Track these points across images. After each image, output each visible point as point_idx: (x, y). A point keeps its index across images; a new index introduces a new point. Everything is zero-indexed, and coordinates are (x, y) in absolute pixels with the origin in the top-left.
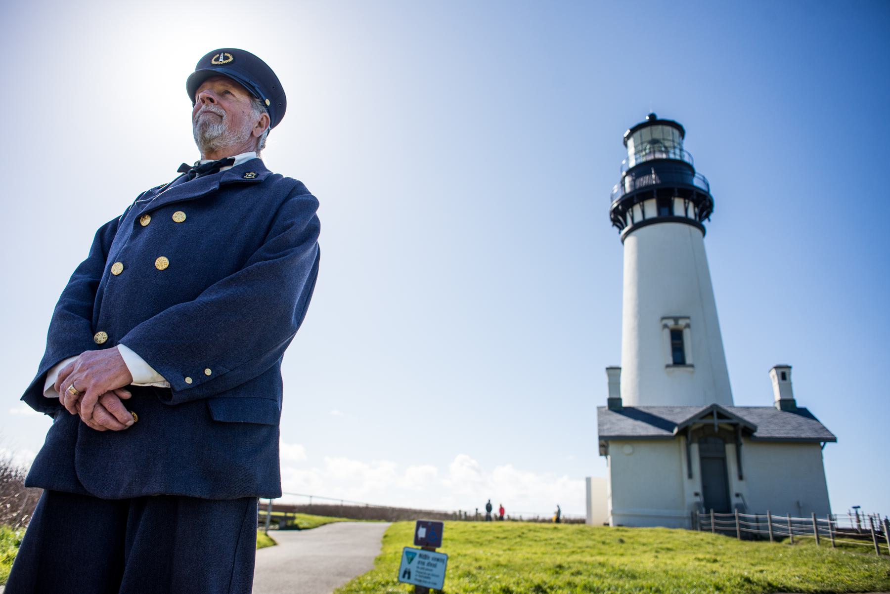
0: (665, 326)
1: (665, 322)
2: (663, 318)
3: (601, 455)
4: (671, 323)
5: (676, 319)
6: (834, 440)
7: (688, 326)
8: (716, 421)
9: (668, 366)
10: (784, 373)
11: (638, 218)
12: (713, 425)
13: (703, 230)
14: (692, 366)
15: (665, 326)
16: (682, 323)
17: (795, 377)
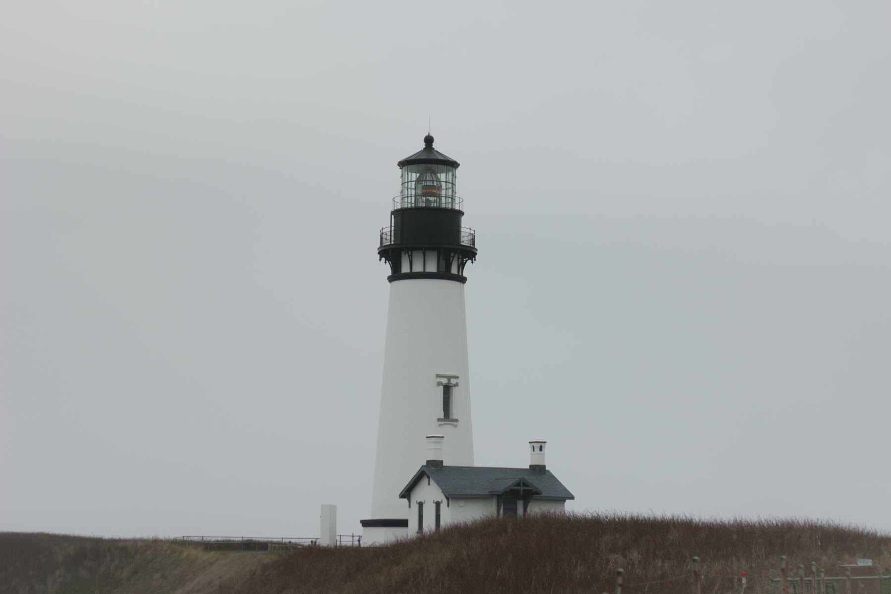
0: (439, 384)
1: (439, 380)
2: (438, 376)
3: (402, 496)
4: (445, 381)
5: (449, 378)
6: (572, 498)
7: (456, 385)
8: (522, 488)
9: (439, 420)
10: (540, 446)
11: (418, 268)
12: (519, 491)
13: (463, 280)
14: (457, 421)
15: (439, 384)
16: (453, 381)
17: (546, 448)
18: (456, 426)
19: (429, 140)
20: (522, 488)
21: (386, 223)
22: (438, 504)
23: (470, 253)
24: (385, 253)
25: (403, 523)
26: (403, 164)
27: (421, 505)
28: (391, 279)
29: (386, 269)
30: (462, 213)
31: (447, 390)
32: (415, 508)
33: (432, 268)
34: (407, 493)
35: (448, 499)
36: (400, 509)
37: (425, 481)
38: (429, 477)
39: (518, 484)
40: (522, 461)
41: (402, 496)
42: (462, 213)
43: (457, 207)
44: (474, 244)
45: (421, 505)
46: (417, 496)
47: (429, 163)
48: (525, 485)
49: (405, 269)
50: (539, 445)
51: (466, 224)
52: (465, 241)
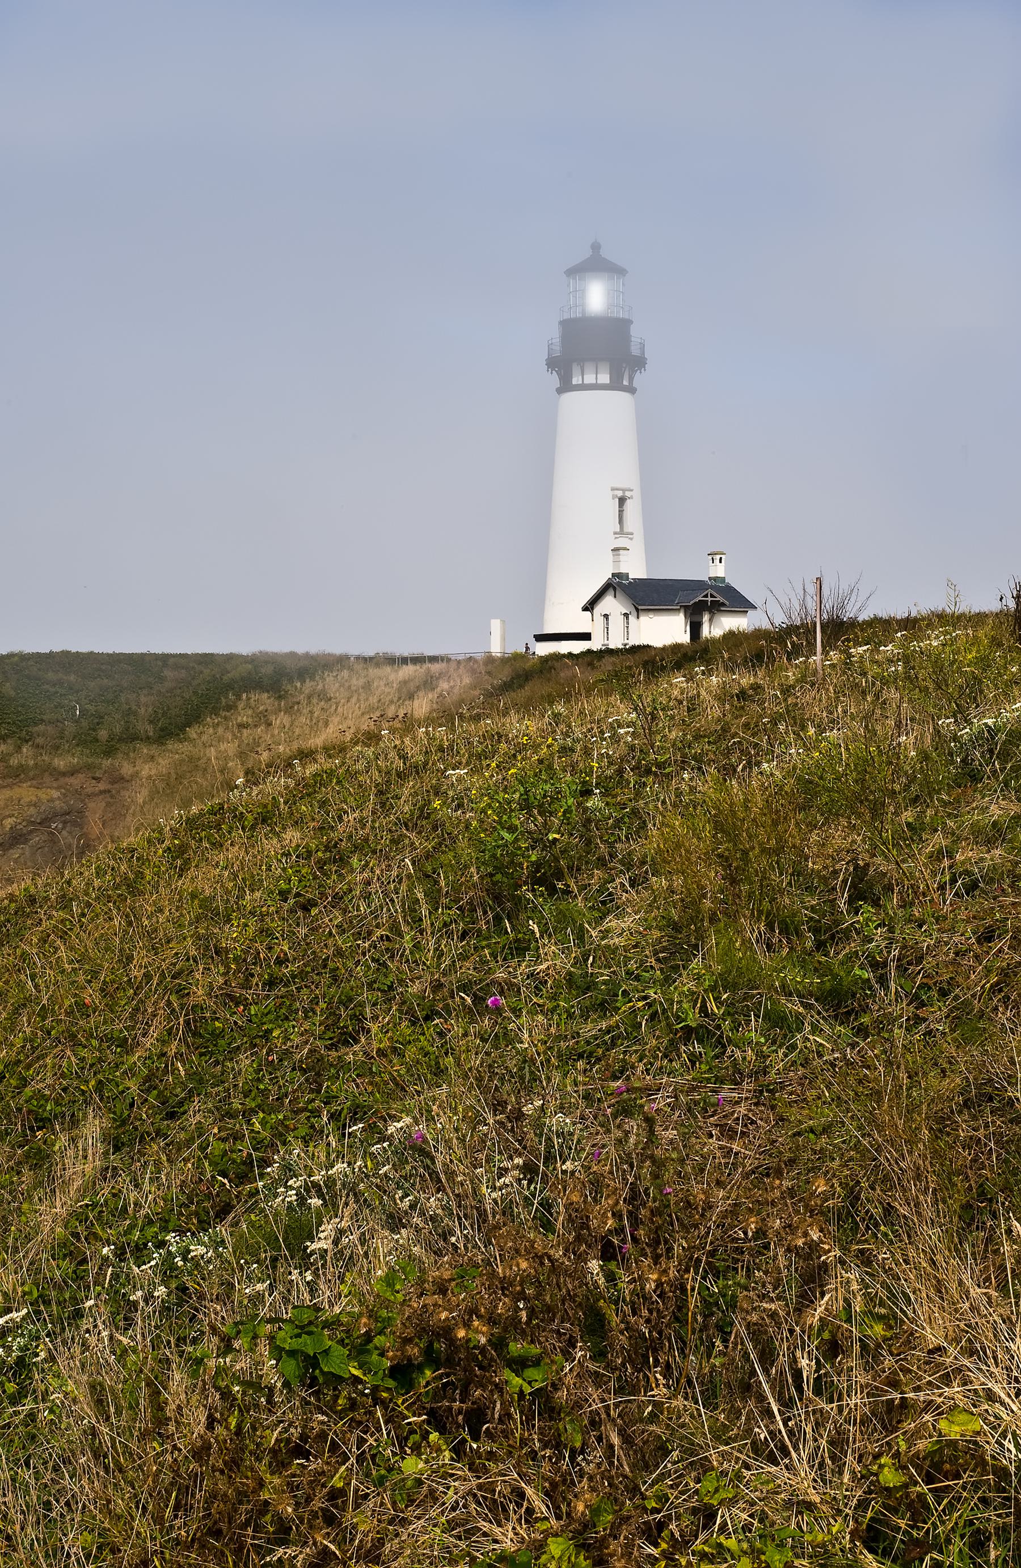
2: (613, 489)
3: (585, 609)
4: (620, 494)
5: (624, 490)
8: (709, 599)
9: (615, 533)
11: (590, 379)
16: (628, 494)
18: (631, 539)
19: (596, 247)
20: (709, 599)
21: (554, 333)
24: (552, 363)
25: (586, 637)
27: (606, 616)
31: (622, 501)
32: (600, 620)
33: (604, 378)
34: (590, 606)
35: (637, 610)
36: (581, 623)
37: (611, 592)
38: (615, 589)
39: (706, 596)
41: (585, 609)
43: (626, 317)
44: (644, 354)
45: (606, 616)
46: (601, 608)
48: (712, 596)
49: (576, 380)
50: (718, 557)
51: (636, 332)
52: (635, 351)
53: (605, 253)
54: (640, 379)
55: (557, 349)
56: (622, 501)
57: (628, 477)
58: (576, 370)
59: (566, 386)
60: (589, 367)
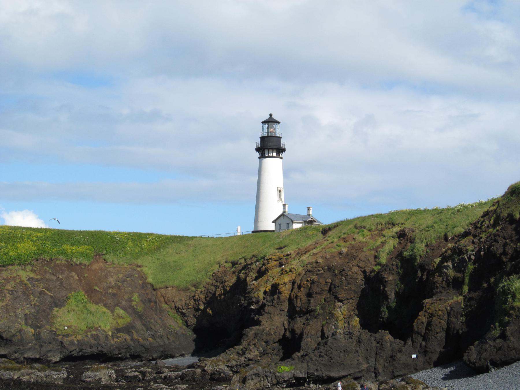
4: (279, 189)
19: (271, 115)
21: (259, 140)
22: (288, 224)
23: (283, 150)
24: (257, 150)
26: (264, 122)
27: (280, 225)
28: (259, 158)
29: (258, 155)
30: (281, 138)
33: (275, 154)
37: (282, 217)
40: (305, 213)
41: (273, 222)
42: (281, 138)
45: (280, 225)
47: (270, 122)
51: (283, 141)
53: (273, 117)
54: (283, 155)
55: (259, 146)
56: (280, 191)
57: (281, 186)
58: (266, 151)
59: (262, 156)
60: (271, 151)
